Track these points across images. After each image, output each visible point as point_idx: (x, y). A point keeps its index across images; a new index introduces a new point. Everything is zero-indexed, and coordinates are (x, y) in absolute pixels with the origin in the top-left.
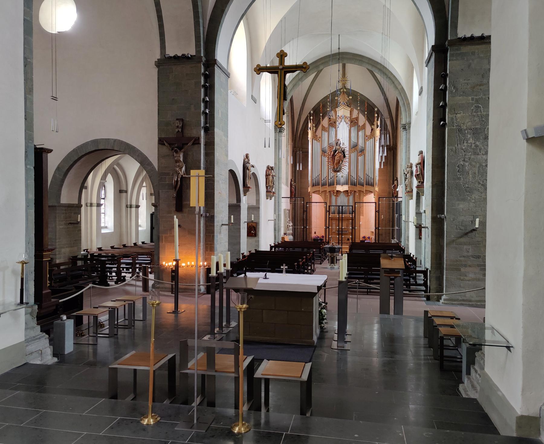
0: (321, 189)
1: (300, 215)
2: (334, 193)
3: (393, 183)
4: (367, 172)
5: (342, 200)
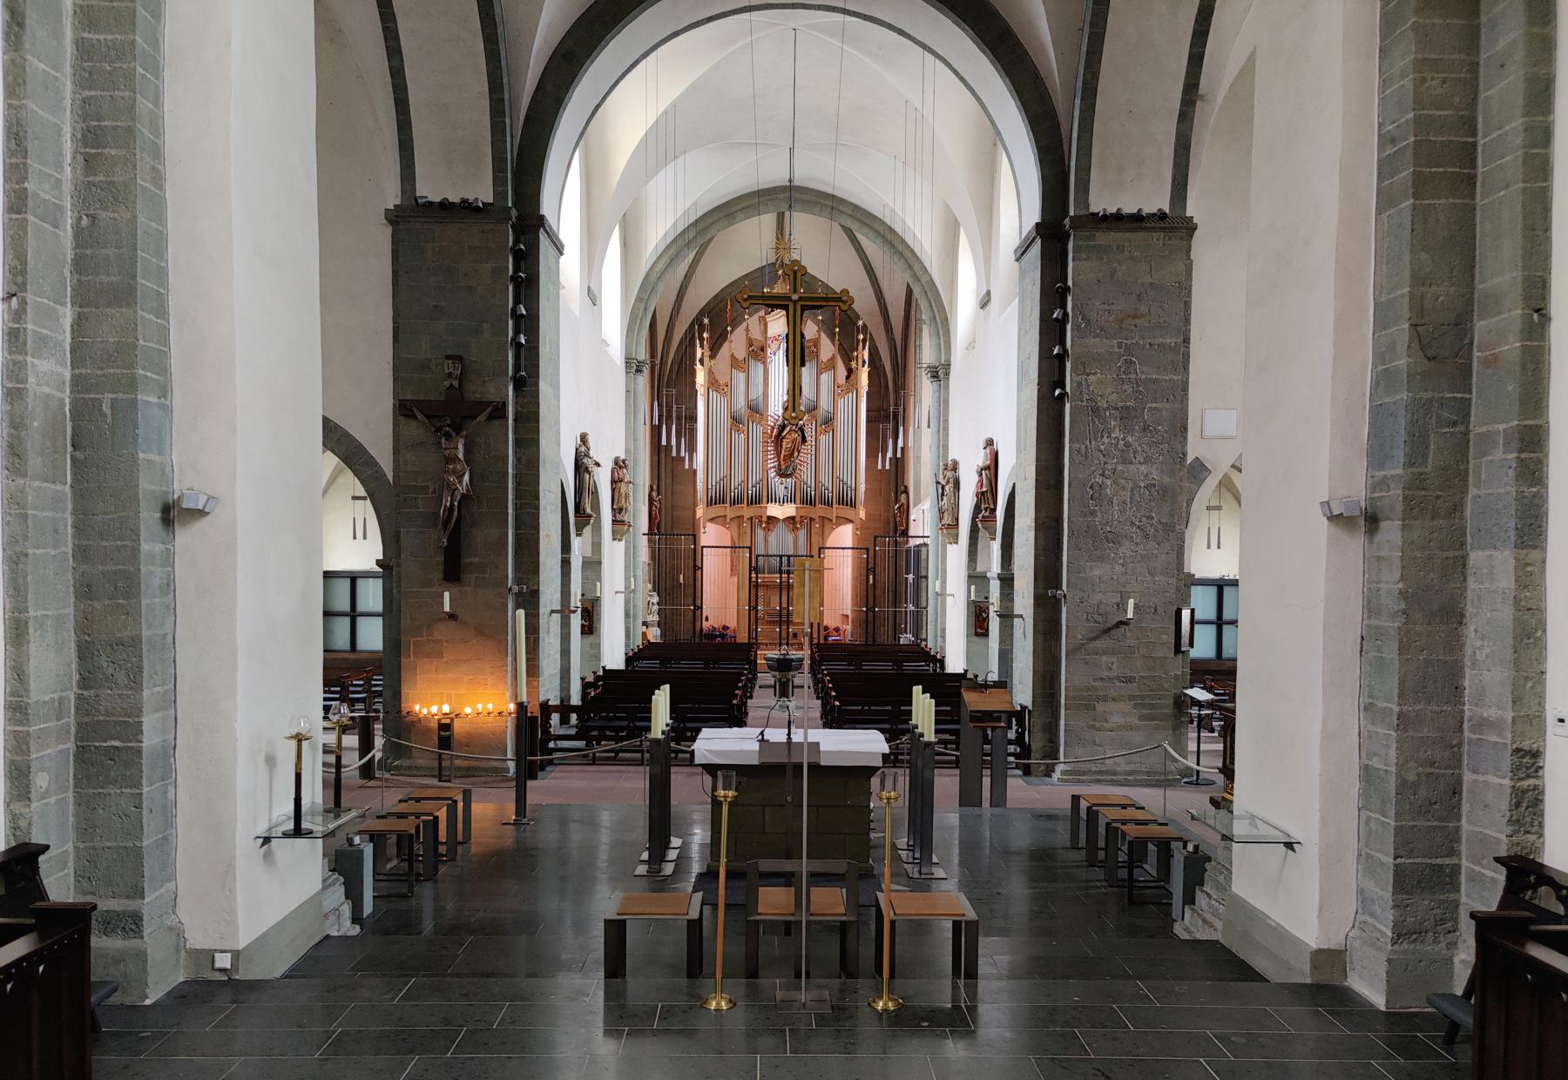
0: (730, 512)
1: (673, 574)
3: (897, 500)
5: (780, 542)
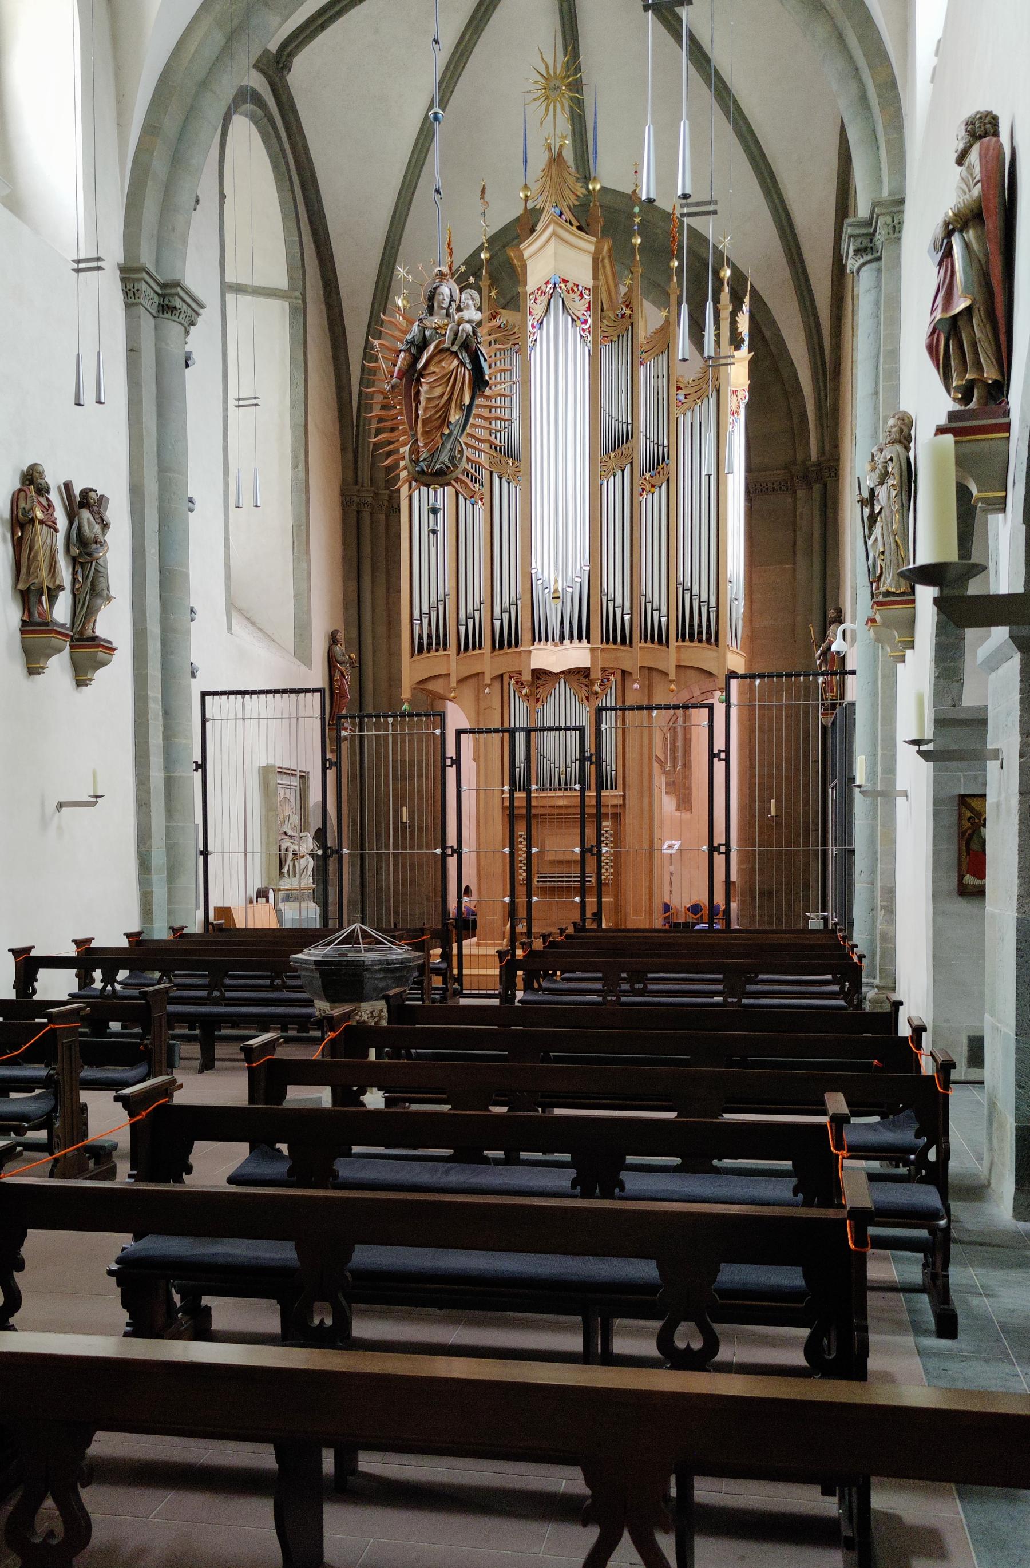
4: (683, 572)
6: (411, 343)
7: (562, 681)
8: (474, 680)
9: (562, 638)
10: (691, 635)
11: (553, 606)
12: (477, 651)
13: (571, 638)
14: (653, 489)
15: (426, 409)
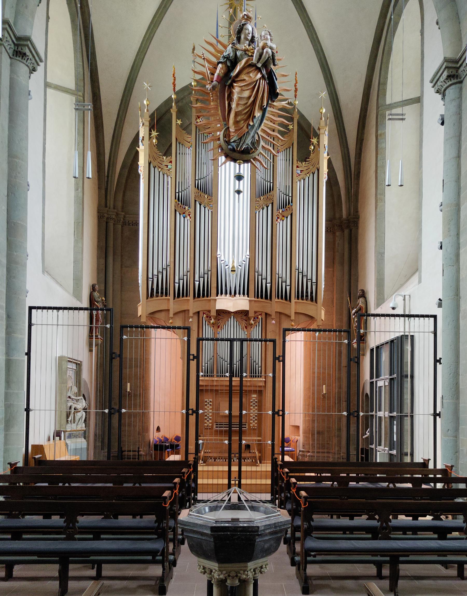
0: (172, 305)
2: (209, 317)
6: (227, 58)
7: (232, 317)
8: (181, 315)
9: (235, 293)
10: (302, 296)
11: (231, 275)
12: (185, 298)
13: (239, 294)
14: (283, 218)
15: (238, 105)
